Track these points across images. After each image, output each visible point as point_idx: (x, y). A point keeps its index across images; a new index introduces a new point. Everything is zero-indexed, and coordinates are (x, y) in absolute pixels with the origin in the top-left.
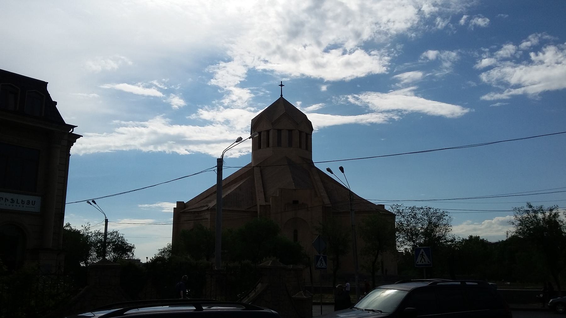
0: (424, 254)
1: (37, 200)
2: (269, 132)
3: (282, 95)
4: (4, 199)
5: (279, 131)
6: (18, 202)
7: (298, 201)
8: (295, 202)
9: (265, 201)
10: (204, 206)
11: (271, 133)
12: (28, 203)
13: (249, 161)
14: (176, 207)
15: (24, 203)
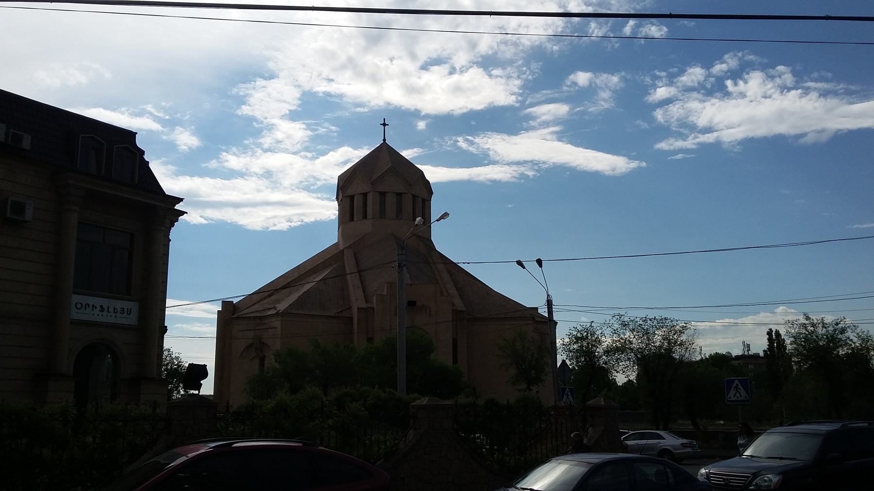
0: (740, 386)
1: (134, 306)
2: (367, 195)
3: (384, 140)
4: (91, 306)
5: (383, 194)
6: (110, 311)
7: (415, 302)
8: (412, 304)
9: (365, 302)
10: (269, 309)
11: (370, 198)
12: (122, 312)
13: (331, 238)
14: (221, 310)
15: (117, 311)
